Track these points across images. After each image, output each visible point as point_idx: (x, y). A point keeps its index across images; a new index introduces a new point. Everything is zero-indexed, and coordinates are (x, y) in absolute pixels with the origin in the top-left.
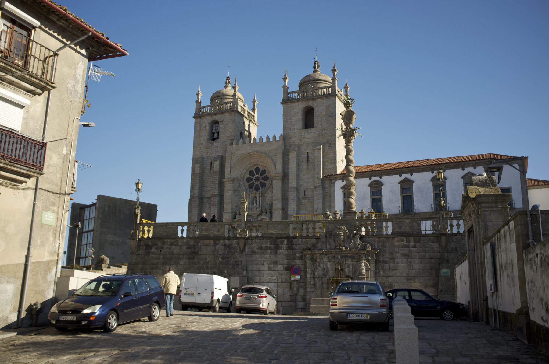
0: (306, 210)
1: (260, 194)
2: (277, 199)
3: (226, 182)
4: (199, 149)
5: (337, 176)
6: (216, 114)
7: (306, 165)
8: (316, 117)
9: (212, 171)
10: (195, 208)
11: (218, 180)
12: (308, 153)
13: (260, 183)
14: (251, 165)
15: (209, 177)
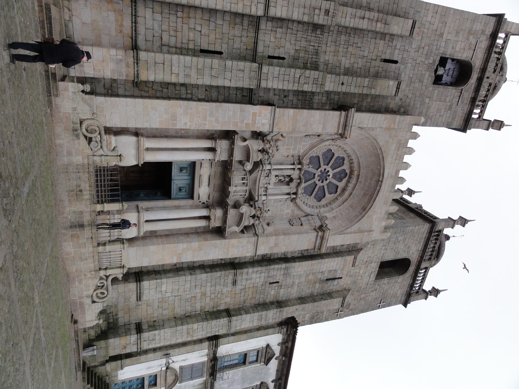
0: (241, 289)
1: (294, 194)
2: (276, 245)
3: (347, 117)
4: (435, 27)
5: (291, 338)
6: (480, 80)
7: (322, 279)
8: (389, 281)
9: (378, 63)
10: (307, 11)
11: (356, 91)
12: (341, 278)
13: (315, 182)
14: (355, 165)
15: (366, 54)
